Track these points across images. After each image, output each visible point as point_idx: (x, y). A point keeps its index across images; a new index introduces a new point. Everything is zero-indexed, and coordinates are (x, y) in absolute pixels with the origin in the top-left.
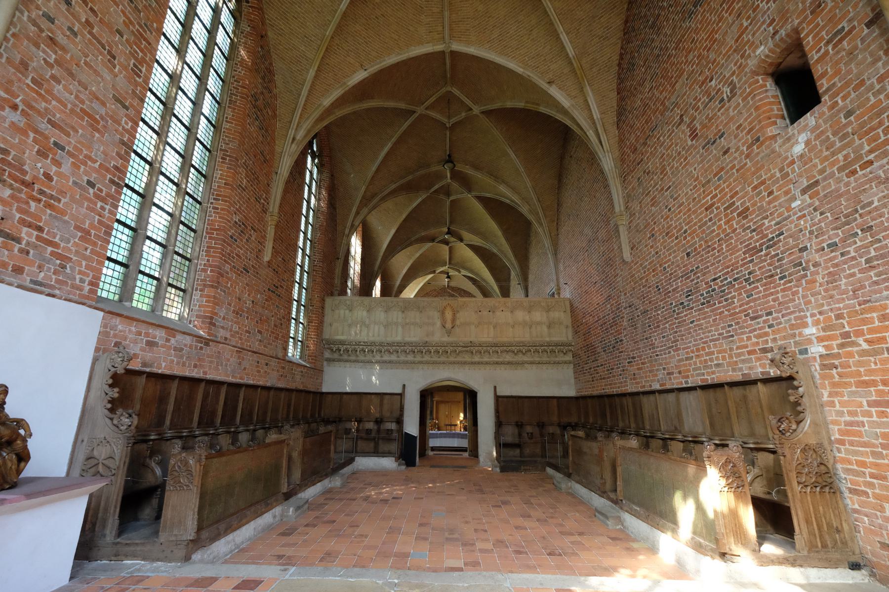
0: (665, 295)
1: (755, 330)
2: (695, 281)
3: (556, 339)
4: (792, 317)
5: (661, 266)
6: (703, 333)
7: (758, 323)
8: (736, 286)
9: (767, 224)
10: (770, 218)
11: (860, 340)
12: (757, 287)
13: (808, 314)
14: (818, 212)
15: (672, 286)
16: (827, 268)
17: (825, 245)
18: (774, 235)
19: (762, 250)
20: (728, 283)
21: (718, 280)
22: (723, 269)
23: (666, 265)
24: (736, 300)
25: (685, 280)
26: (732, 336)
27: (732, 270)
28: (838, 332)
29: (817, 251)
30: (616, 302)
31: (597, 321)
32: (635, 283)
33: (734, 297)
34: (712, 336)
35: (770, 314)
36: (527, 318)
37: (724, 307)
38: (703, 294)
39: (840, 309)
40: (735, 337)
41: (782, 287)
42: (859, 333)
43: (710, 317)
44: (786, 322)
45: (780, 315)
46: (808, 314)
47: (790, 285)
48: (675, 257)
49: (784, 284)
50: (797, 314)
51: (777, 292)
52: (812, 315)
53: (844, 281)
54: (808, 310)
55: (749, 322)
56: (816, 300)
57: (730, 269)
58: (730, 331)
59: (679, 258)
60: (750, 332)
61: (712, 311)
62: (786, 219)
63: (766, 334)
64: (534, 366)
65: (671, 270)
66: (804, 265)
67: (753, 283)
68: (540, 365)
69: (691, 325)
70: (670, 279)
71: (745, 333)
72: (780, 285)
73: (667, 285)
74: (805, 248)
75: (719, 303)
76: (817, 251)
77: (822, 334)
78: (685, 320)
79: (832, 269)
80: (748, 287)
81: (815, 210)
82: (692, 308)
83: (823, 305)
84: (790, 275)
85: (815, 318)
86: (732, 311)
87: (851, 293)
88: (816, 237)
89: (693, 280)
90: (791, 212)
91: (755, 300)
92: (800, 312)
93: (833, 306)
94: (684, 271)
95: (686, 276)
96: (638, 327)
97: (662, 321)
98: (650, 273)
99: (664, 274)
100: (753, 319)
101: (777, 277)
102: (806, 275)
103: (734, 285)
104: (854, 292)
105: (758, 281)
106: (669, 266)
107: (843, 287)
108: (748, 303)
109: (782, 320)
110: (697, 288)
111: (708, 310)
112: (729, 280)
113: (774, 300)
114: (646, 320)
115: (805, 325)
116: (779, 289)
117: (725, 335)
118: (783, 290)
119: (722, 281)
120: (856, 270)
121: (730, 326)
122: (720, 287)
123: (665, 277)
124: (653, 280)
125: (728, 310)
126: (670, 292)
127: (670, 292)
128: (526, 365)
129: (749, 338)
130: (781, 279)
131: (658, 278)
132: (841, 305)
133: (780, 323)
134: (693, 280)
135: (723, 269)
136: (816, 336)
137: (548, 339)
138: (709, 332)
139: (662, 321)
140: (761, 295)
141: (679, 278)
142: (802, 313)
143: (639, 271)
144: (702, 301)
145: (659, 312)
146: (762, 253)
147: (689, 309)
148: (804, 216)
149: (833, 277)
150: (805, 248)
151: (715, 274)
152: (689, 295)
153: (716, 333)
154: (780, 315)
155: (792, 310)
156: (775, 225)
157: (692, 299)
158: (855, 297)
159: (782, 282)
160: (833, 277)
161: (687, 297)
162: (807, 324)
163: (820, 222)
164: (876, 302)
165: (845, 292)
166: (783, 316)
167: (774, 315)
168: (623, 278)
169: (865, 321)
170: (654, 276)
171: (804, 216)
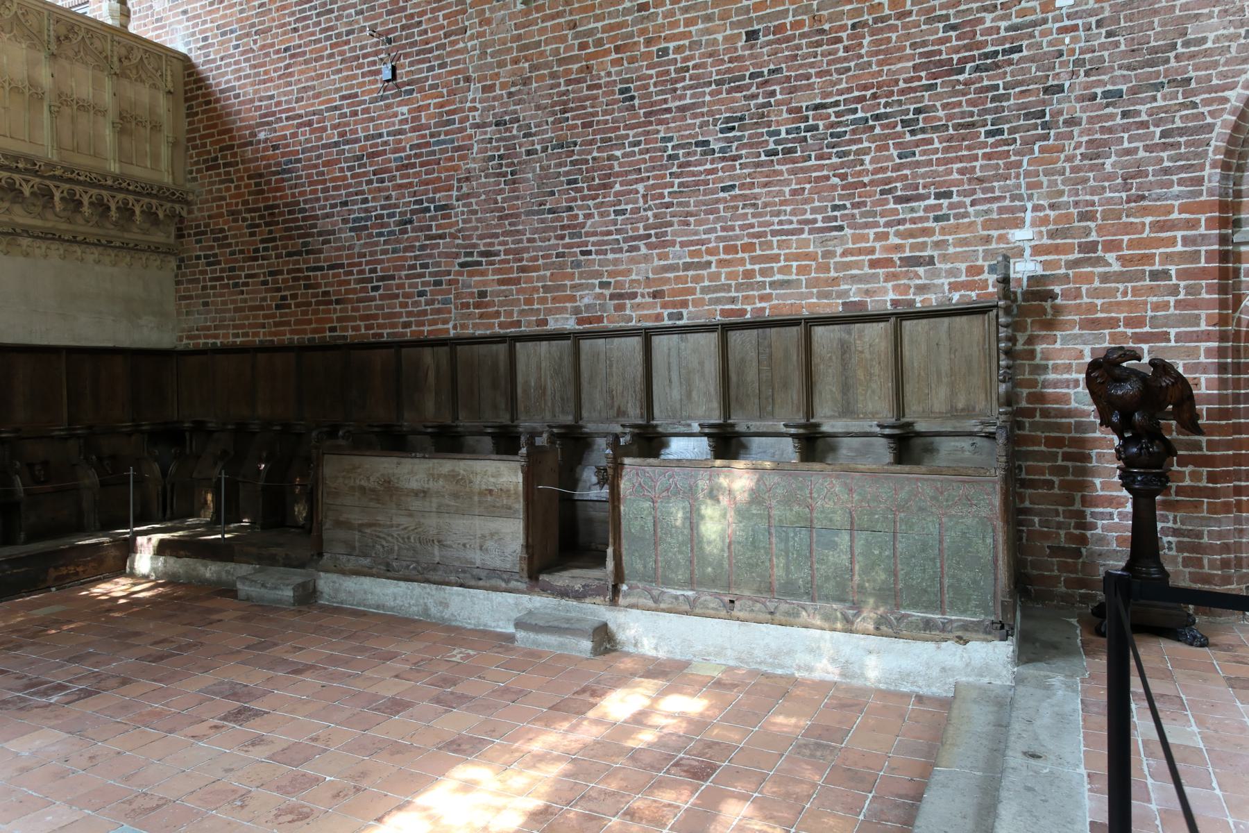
0: (647, 115)
1: (900, 222)
2: (761, 100)
3: (141, 172)
4: (995, 206)
5: (649, 42)
6: (754, 216)
7: (912, 210)
8: (878, 131)
9: (988, 24)
10: (999, 12)
11: (1111, 257)
12: (930, 141)
13: (1029, 205)
14: (1103, 31)
15: (682, 97)
16: (1089, 131)
17: (1099, 91)
18: (1000, 48)
19: (962, 71)
20: (854, 122)
21: (830, 111)
22: (850, 90)
23: (671, 45)
24: (867, 158)
25: (728, 92)
26: (841, 228)
27: (874, 96)
28: (1076, 241)
29: (1081, 99)
30: (442, 105)
31: (336, 144)
32: (534, 68)
33: (866, 151)
34: (780, 223)
35: (948, 195)
36: (44, 75)
37: (834, 167)
38: (778, 133)
39: (1093, 204)
40: (848, 231)
41: (988, 150)
42: (1111, 246)
43: (787, 183)
44: (977, 214)
45: (968, 200)
46: (1029, 205)
47: (1006, 148)
48: (708, 31)
49: (994, 145)
50: (1007, 203)
51: (976, 158)
52: (1036, 208)
53: (1114, 158)
54: (1030, 197)
55: (892, 206)
56: (1053, 184)
57: (868, 93)
58: (835, 219)
59: (720, 37)
60: (887, 224)
61: (792, 172)
62: (1034, 24)
63: (926, 232)
64: (56, 249)
65: (685, 60)
66: (1047, 118)
67: (923, 130)
68: (78, 250)
69: (722, 195)
70: (676, 81)
71: (876, 225)
72: (985, 145)
73: (662, 92)
74: (1060, 88)
75: (819, 158)
76: (1081, 99)
77: (1046, 241)
78: (706, 183)
79: (1098, 136)
80: (908, 137)
81: (1099, 24)
82: (734, 158)
83: (1061, 193)
84: (1013, 131)
85: (1042, 214)
86: (850, 180)
87: (1120, 181)
88: (1087, 74)
89: (754, 96)
90: (1050, 15)
91: (918, 164)
92: (1012, 201)
93: (1081, 198)
94: (729, 70)
95: (733, 82)
96: (526, 180)
97: (618, 175)
98: (608, 52)
99: (659, 64)
100: (899, 200)
101: (982, 130)
102: (1046, 137)
103: (873, 128)
104: (1125, 179)
105: (935, 129)
106: (678, 49)
107: (1108, 168)
108: (897, 168)
109: (970, 209)
110: (763, 116)
111: (784, 168)
112: (860, 115)
113: (961, 172)
114: (560, 165)
115: (1019, 224)
116: (980, 152)
117: (819, 224)
118: (987, 156)
119: (838, 114)
120: (1140, 144)
121: (835, 208)
122: (832, 125)
123: (659, 75)
124: (608, 70)
125: (843, 177)
126: (669, 110)
127: (669, 110)
128: (25, 242)
129: (882, 237)
130: (989, 134)
131: (628, 71)
132: (1096, 198)
133: (966, 215)
134: (754, 96)
135: (850, 90)
136: (1033, 243)
137: (114, 167)
138: (778, 214)
139: (618, 175)
140: (934, 157)
141: (710, 84)
142: (1017, 203)
143: (563, 39)
144: (772, 146)
145: (618, 153)
146: (961, 77)
147: (723, 159)
148: (1075, 28)
149: (1096, 150)
150: (1060, 88)
151: (826, 95)
152: (733, 128)
153: (795, 219)
154: (968, 200)
155: (997, 194)
156: (1007, 30)
157: (740, 138)
158: (1126, 187)
159: (991, 140)
160: (1096, 150)
161: (722, 131)
162: (1023, 221)
163: (1103, 47)
164: (1158, 199)
165: (1110, 177)
166: (973, 204)
167: (955, 199)
168: (484, 46)
169: (1129, 228)
170: (615, 62)
171: (1075, 28)
